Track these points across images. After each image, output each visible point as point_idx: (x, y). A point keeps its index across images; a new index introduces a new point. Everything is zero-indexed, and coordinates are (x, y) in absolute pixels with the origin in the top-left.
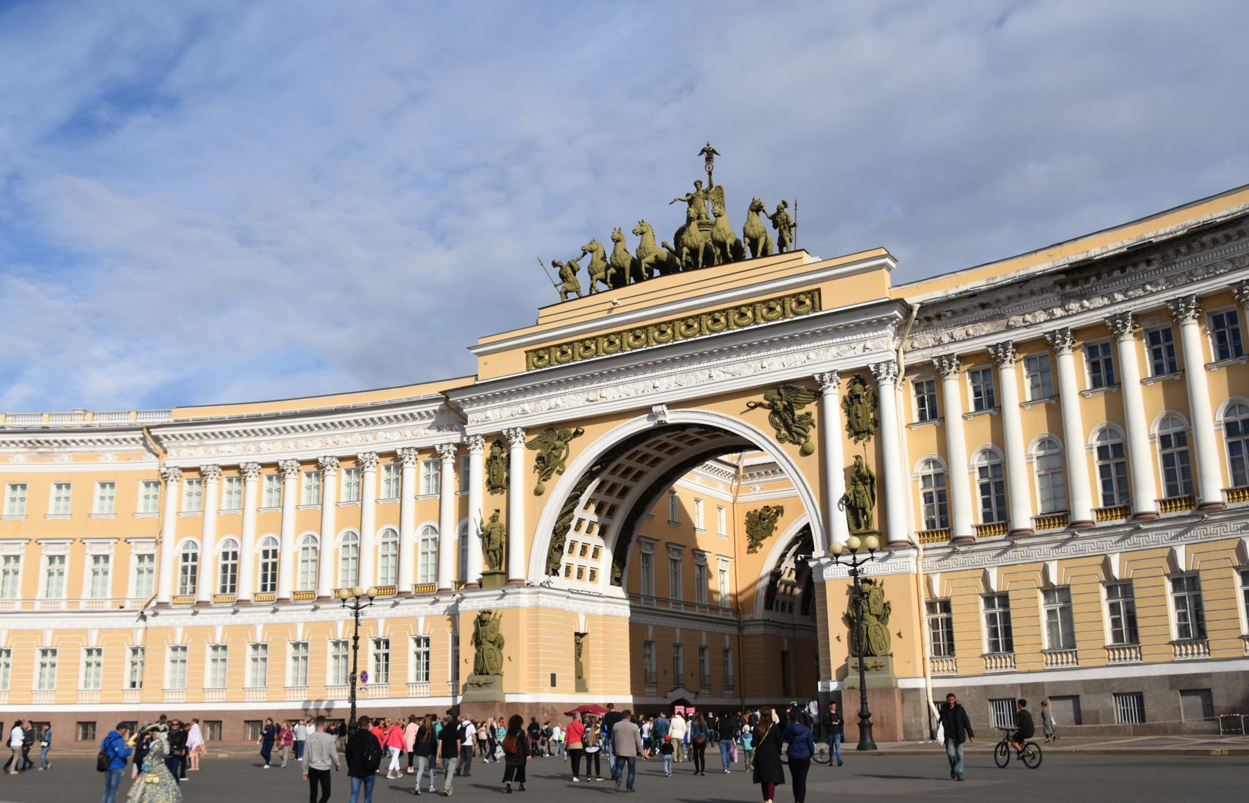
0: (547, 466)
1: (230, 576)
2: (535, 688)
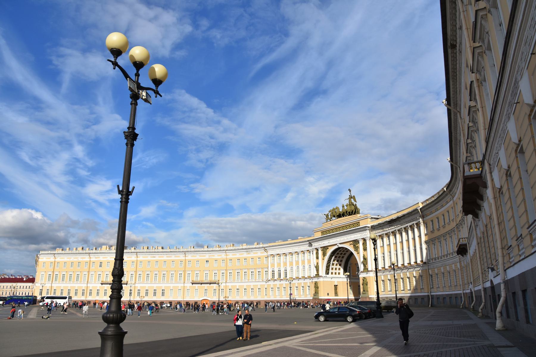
0: (324, 254)
1: (280, 275)
2: (324, 296)
